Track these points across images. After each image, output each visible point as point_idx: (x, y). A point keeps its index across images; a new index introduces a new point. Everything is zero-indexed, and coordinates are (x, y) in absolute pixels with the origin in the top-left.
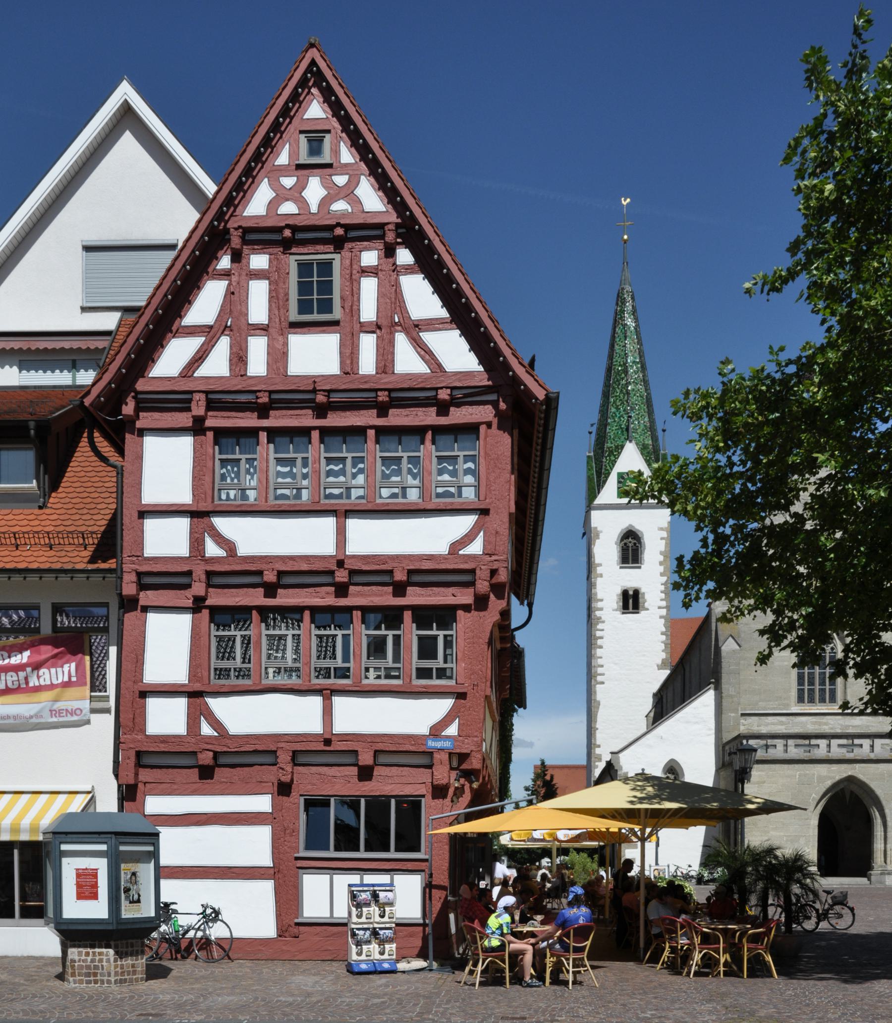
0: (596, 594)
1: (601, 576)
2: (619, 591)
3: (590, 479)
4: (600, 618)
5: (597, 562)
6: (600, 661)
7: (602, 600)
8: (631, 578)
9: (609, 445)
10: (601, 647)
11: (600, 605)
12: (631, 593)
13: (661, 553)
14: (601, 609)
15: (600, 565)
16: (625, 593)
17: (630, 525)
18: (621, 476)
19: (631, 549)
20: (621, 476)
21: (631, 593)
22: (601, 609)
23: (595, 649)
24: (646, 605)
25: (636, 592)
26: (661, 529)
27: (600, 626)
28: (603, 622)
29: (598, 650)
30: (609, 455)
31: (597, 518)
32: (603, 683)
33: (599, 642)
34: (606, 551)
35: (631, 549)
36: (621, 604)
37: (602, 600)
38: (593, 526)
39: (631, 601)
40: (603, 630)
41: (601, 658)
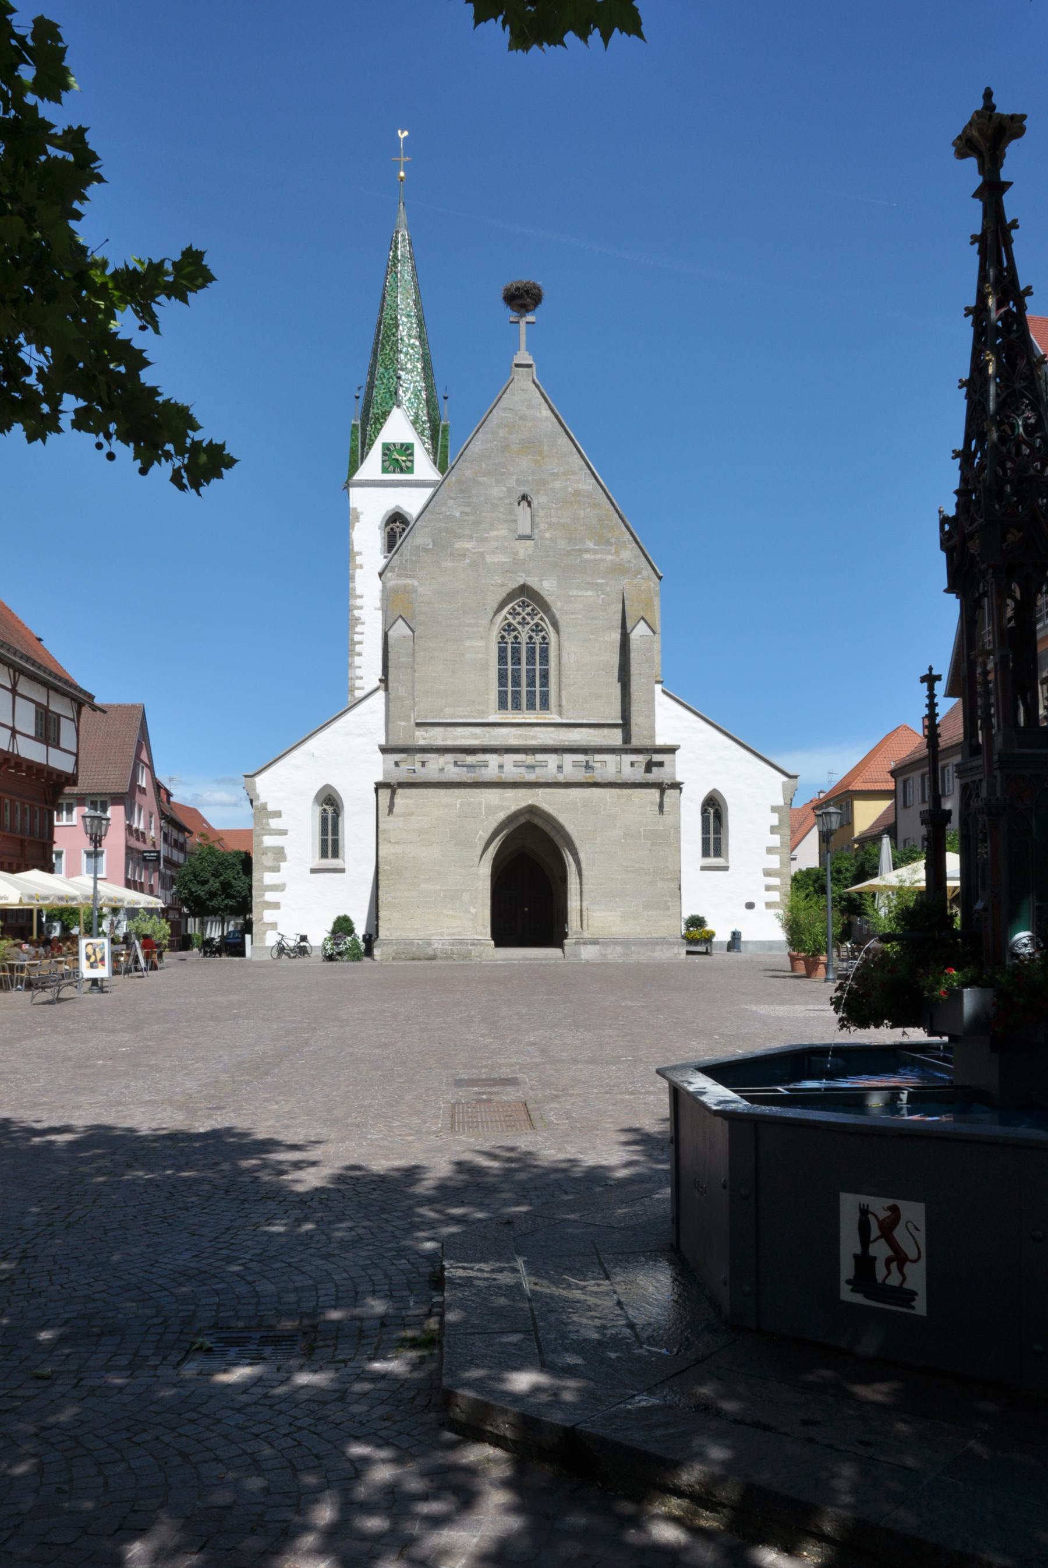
0: (354, 589)
1: (361, 567)
4: (359, 618)
5: (356, 549)
6: (358, 672)
7: (361, 597)
9: (376, 411)
10: (360, 654)
11: (358, 602)
14: (361, 608)
15: (360, 554)
22: (361, 608)
23: (353, 656)
27: (358, 629)
28: (363, 623)
29: (357, 658)
30: (375, 423)
33: (358, 648)
34: (367, 539)
37: (361, 597)
38: (352, 505)
40: (362, 633)
41: (360, 667)
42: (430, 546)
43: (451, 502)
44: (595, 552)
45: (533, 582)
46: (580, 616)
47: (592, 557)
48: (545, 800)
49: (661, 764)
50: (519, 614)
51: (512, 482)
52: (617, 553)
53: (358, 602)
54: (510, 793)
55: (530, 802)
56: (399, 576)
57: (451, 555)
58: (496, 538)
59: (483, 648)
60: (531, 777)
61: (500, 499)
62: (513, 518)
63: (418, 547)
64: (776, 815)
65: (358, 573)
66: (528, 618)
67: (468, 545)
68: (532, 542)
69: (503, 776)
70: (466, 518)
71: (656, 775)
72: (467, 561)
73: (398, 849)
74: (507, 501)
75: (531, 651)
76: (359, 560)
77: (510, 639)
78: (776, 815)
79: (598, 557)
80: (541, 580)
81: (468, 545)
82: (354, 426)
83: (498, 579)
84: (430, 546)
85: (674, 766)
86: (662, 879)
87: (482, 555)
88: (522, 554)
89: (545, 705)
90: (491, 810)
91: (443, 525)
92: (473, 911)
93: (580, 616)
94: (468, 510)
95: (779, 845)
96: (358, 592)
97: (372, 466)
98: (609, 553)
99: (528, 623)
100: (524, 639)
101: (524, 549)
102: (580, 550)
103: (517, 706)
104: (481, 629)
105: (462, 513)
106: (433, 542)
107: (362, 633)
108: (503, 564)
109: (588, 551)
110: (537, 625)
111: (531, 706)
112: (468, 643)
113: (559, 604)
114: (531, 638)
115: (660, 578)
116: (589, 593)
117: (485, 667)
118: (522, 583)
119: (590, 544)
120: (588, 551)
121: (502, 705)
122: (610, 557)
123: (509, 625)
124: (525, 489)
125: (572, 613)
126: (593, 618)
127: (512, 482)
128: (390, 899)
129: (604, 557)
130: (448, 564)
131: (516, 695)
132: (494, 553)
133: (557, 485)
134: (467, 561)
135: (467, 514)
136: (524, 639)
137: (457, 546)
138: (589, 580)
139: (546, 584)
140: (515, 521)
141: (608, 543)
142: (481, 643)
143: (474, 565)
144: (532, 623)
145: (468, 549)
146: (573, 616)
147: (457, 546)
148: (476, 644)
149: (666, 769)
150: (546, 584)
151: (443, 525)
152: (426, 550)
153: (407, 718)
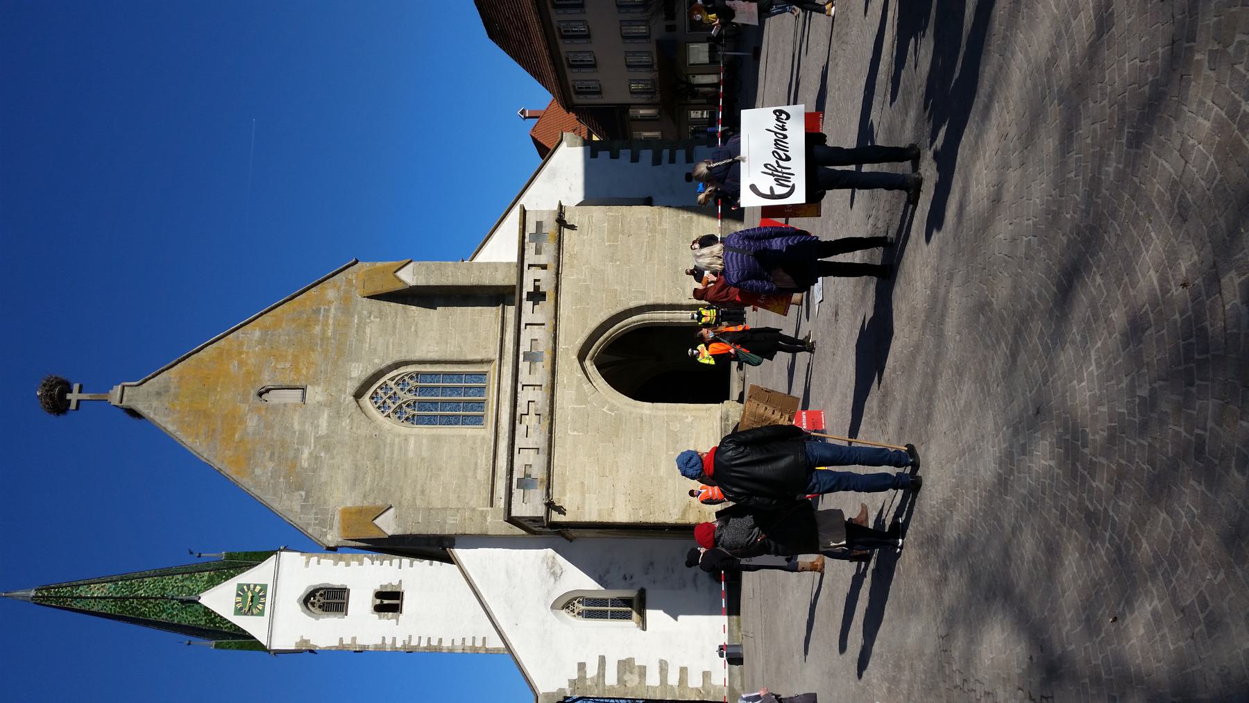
1: (354, 639)
2: (376, 616)
3: (241, 647)
6: (458, 643)
8: (361, 602)
10: (440, 640)
11: (389, 642)
12: (378, 602)
13: (336, 564)
14: (394, 639)
15: (341, 639)
16: (379, 609)
18: (238, 612)
19: (329, 600)
20: (238, 612)
21: (378, 602)
22: (394, 639)
24: (395, 583)
25: (379, 595)
26: (307, 563)
31: (283, 641)
34: (326, 632)
35: (329, 600)
39: (389, 601)
42: (303, 493)
43: (258, 471)
44: (326, 324)
45: (352, 386)
47: (331, 327)
48: (573, 335)
49: (539, 225)
51: (244, 407)
52: (330, 302)
53: (389, 642)
54: (562, 378)
55: (575, 357)
56: (331, 528)
58: (302, 423)
59: (418, 439)
60: (547, 357)
61: (259, 419)
64: (600, 153)
65: (359, 642)
66: (390, 393)
67: (306, 455)
71: (550, 227)
73: (621, 499)
75: (422, 390)
76: (347, 641)
77: (410, 411)
78: (600, 153)
79: (331, 321)
81: (306, 455)
82: (216, 646)
84: (303, 493)
85: (542, 212)
86: (660, 224)
87: (318, 439)
88: (320, 397)
90: (581, 398)
92: (689, 420)
94: (268, 453)
95: (629, 151)
96: (380, 642)
97: (253, 626)
98: (327, 311)
100: (411, 397)
101: (316, 394)
102: (322, 340)
103: (481, 404)
108: (330, 417)
109: (324, 331)
110: (397, 384)
112: (411, 454)
113: (377, 361)
114: (410, 391)
115: (357, 262)
116: (368, 330)
117: (437, 439)
119: (317, 329)
120: (324, 331)
121: (478, 421)
123: (395, 412)
124: (253, 392)
126: (394, 327)
128: (676, 510)
130: (324, 475)
132: (318, 426)
133: (252, 361)
135: (272, 454)
136: (411, 397)
137: (305, 465)
138: (354, 331)
139: (355, 374)
140: (285, 405)
141: (317, 311)
142: (412, 441)
143: (328, 448)
145: (311, 454)
148: (412, 446)
149: (544, 219)
150: (355, 374)
152: (306, 500)
153: (484, 515)
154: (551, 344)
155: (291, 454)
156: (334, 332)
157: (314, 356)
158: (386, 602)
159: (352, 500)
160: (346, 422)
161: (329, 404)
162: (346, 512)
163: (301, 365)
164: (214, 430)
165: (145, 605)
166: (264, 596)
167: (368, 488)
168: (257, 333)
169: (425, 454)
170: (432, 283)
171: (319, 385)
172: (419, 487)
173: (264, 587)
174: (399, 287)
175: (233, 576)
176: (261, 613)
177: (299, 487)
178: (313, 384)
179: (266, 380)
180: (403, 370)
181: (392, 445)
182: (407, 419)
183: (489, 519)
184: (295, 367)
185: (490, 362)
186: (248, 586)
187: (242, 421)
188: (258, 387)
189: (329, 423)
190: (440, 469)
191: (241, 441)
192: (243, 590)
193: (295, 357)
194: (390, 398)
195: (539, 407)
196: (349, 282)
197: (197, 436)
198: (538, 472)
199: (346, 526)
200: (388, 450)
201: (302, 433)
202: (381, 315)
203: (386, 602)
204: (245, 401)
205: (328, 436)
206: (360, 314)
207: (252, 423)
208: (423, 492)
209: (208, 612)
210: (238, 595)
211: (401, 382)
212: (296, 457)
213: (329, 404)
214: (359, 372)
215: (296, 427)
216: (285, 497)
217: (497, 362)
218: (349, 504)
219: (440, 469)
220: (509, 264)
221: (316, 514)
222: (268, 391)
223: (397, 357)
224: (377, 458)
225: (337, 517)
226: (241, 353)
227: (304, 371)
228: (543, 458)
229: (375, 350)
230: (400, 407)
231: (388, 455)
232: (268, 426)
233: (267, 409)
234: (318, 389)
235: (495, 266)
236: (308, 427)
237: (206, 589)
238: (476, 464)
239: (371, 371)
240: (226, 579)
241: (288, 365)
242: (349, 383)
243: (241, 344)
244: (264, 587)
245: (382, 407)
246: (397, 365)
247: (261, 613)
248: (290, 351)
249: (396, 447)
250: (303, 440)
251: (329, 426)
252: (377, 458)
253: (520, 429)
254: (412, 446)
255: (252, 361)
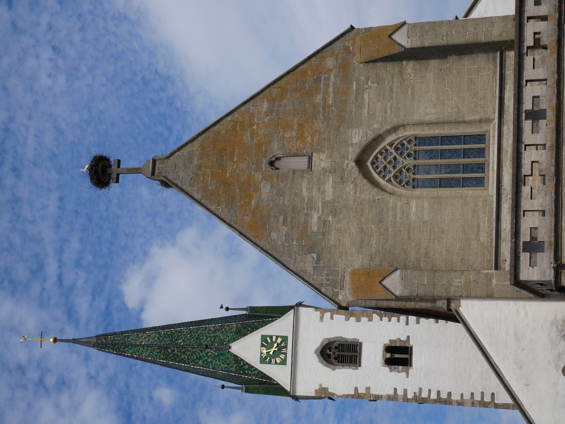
2: (387, 369)
7: (395, 390)
8: (372, 355)
10: (450, 394)
12: (388, 355)
13: (347, 319)
14: (405, 391)
16: (390, 362)
17: (316, 352)
18: (263, 360)
19: (340, 353)
20: (263, 360)
21: (388, 355)
25: (389, 349)
26: (322, 318)
32: (493, 394)
35: (340, 353)
36: (401, 367)
37: (395, 390)
39: (398, 356)
40: (430, 391)
42: (315, 255)
43: (274, 235)
44: (326, 92)
45: (353, 153)
46: (389, 105)
47: (331, 95)
50: (385, 167)
51: (258, 176)
56: (342, 288)
57: (324, 234)
58: (310, 190)
61: (272, 186)
62: (291, 174)
63: (315, 268)
67: (315, 219)
68: (314, 154)
69: (548, 144)
70: (289, 219)
72: (330, 218)
74: (275, 180)
79: (331, 89)
80: (352, 145)
81: (315, 219)
83: (350, 187)
84: (315, 255)
87: (325, 204)
88: (325, 164)
89: (481, 138)
91: (295, 243)
93: (389, 105)
94: (281, 218)
98: (328, 79)
99: (395, 158)
100: (410, 162)
101: (321, 161)
102: (324, 108)
103: (481, 168)
104: (399, 204)
105: (284, 224)
106: (310, 253)
107: (430, 391)
109: (325, 100)
110: (397, 149)
111: (481, 153)
112: (413, 217)
113: (376, 126)
114: (409, 155)
116: (366, 96)
118: (354, 164)
119: (319, 98)
120: (325, 100)
122: (332, 78)
123: (395, 177)
124: (265, 162)
125: (386, 112)
127: (258, 176)
129: (331, 84)
130: (333, 238)
131: (466, 168)
132: (323, 192)
134: (330, 218)
135: (285, 219)
136: (410, 162)
137: (315, 229)
138: (353, 97)
139: (356, 140)
140: (294, 172)
142: (413, 203)
143: (334, 212)
144: (394, 154)
145: (319, 218)
146: (389, 111)
147: (315, 229)
148: (414, 210)
150: (356, 140)
151: (295, 243)
154: (554, 101)
155: (302, 219)
156: (334, 100)
157: (319, 125)
158: (397, 356)
159: (358, 261)
160: (350, 187)
161: (333, 171)
162: (354, 273)
163: (306, 134)
164: (233, 198)
165: (184, 353)
166: (286, 347)
167: (373, 250)
168: (265, 105)
169: (426, 217)
170: (427, 44)
171: (324, 152)
172: (423, 250)
173: (285, 339)
174: (395, 50)
175: (257, 328)
176: (284, 362)
177: (311, 251)
178: (318, 151)
179: (276, 149)
180: (402, 133)
181: (394, 209)
182: (407, 183)
183: (494, 282)
184: (301, 137)
185: (488, 121)
186: (271, 337)
187: (257, 190)
188: (270, 156)
189: (334, 188)
190: (442, 232)
191: (257, 207)
192: (266, 341)
193: (300, 125)
194: (390, 162)
195: (543, 167)
196: (347, 49)
197: (219, 203)
198: (545, 235)
199: (356, 289)
200: (390, 214)
201: (310, 199)
202: (378, 80)
203: (397, 356)
204: (259, 169)
205: (334, 201)
206: (357, 80)
207: (265, 190)
208: (427, 254)
209: (237, 359)
210: (262, 345)
211: (400, 148)
212: (306, 222)
213: (333, 171)
214: (358, 138)
215: (305, 193)
216: (298, 259)
217: (496, 121)
218: (357, 266)
219: (442, 232)
220: (505, 18)
221: (328, 275)
222: (278, 159)
223: (395, 122)
224: (380, 222)
225: (348, 279)
226: (252, 124)
227: (309, 139)
228: (549, 221)
229: (374, 115)
230: (400, 171)
231: (391, 218)
232: (280, 193)
233: (278, 177)
234: (323, 156)
235: (491, 21)
236: (315, 193)
237: (234, 340)
238: (479, 227)
239: (371, 136)
240: (251, 332)
241: (294, 134)
242: (350, 149)
243: (252, 116)
244: (285, 339)
245: (383, 173)
246: (395, 129)
247: (284, 362)
248: (295, 121)
249: (399, 211)
250: (311, 206)
251: (334, 192)
252: (380, 222)
253: (525, 190)
254: (414, 210)
255: (261, 132)
